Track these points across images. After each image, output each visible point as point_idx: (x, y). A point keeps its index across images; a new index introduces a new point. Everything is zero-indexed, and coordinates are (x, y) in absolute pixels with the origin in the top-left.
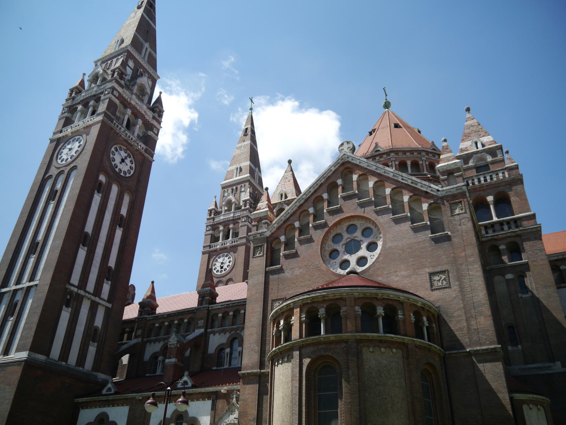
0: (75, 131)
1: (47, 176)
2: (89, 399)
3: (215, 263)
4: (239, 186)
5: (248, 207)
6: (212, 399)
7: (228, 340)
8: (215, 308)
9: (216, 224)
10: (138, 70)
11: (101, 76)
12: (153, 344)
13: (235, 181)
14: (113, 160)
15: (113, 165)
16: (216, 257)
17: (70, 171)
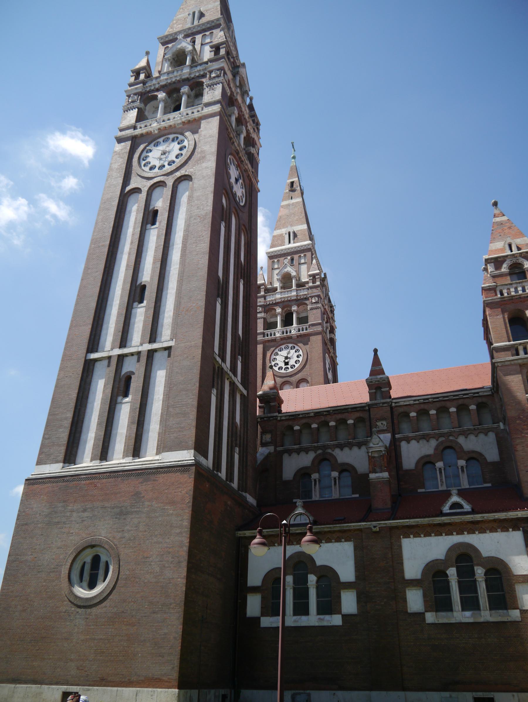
0: (166, 127)
1: (128, 188)
2: (267, 532)
3: (275, 357)
4: (296, 257)
5: (318, 283)
6: (521, 529)
7: (436, 449)
8: (402, 403)
9: (269, 305)
11: (191, 53)
12: (294, 455)
13: (285, 249)
16: (275, 349)
17: (177, 183)
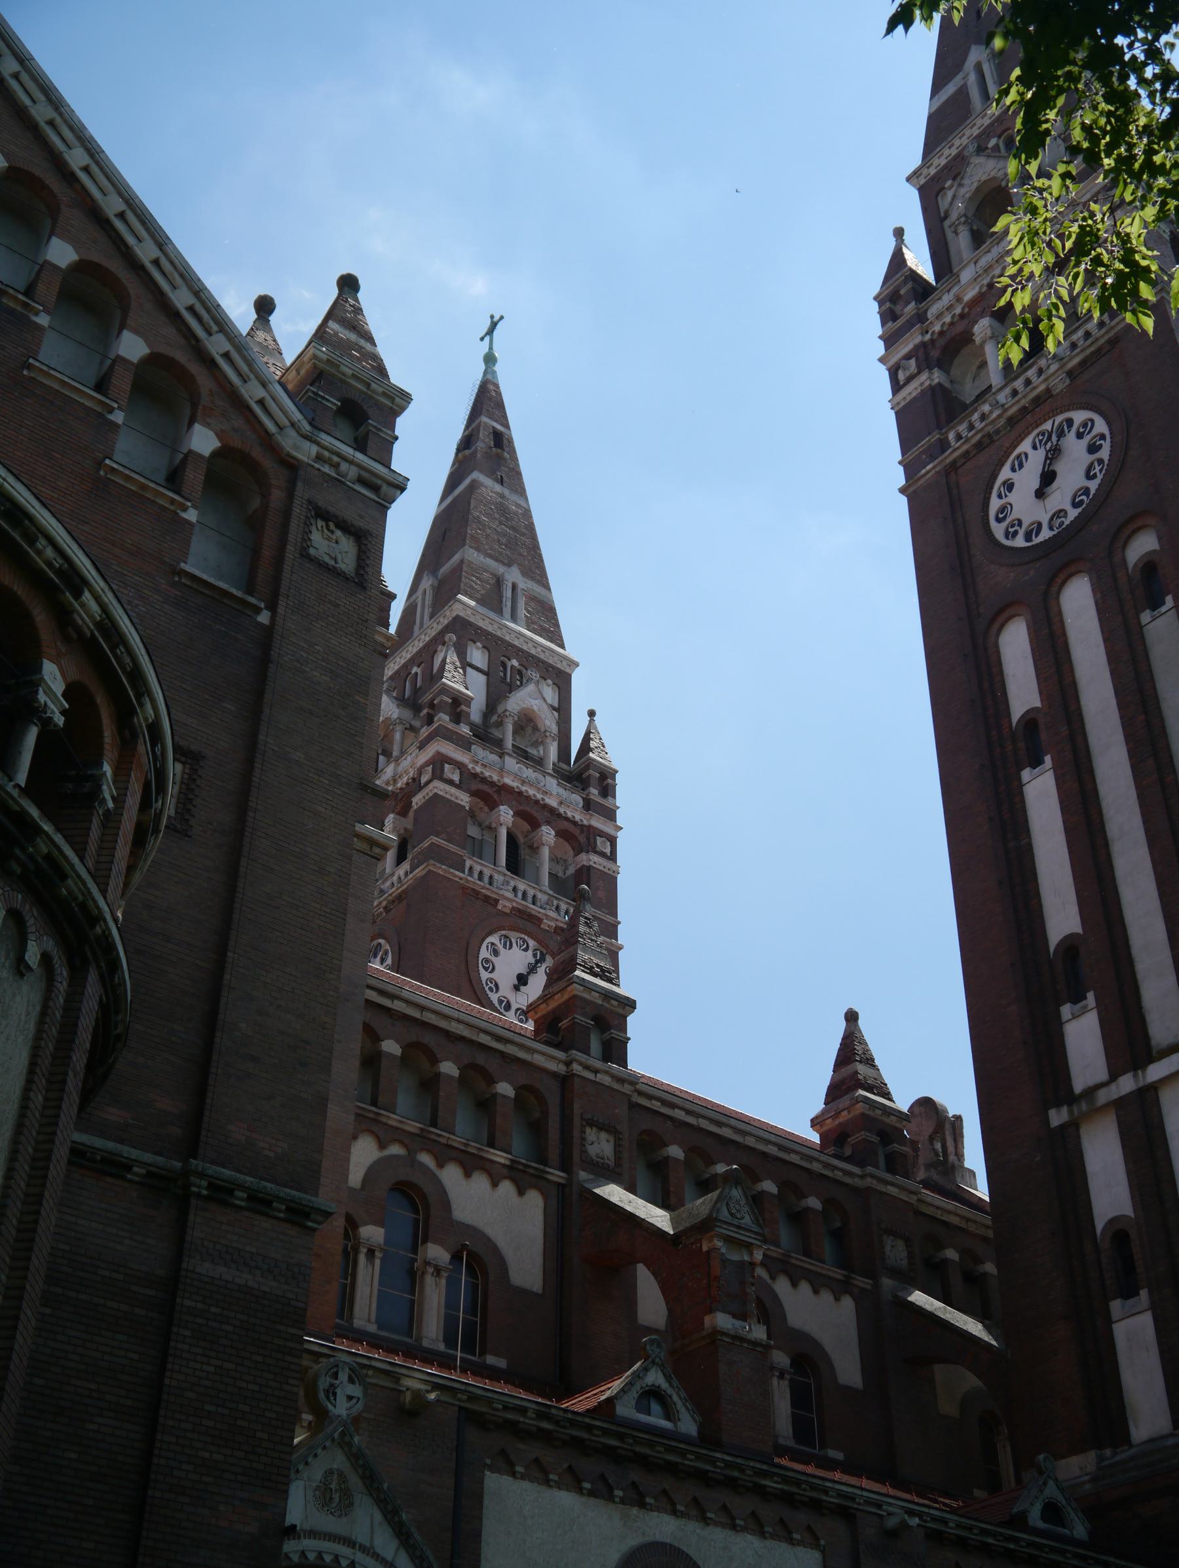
10: (504, 665)
14: (491, 989)
15: (497, 1005)
